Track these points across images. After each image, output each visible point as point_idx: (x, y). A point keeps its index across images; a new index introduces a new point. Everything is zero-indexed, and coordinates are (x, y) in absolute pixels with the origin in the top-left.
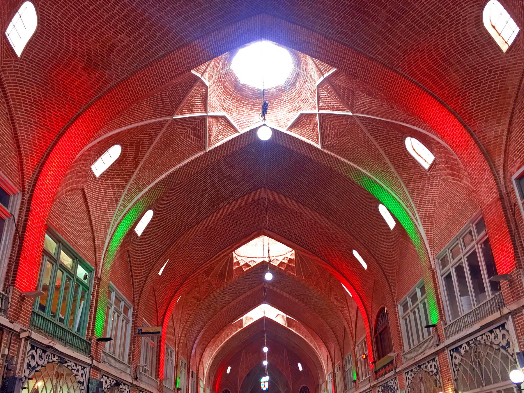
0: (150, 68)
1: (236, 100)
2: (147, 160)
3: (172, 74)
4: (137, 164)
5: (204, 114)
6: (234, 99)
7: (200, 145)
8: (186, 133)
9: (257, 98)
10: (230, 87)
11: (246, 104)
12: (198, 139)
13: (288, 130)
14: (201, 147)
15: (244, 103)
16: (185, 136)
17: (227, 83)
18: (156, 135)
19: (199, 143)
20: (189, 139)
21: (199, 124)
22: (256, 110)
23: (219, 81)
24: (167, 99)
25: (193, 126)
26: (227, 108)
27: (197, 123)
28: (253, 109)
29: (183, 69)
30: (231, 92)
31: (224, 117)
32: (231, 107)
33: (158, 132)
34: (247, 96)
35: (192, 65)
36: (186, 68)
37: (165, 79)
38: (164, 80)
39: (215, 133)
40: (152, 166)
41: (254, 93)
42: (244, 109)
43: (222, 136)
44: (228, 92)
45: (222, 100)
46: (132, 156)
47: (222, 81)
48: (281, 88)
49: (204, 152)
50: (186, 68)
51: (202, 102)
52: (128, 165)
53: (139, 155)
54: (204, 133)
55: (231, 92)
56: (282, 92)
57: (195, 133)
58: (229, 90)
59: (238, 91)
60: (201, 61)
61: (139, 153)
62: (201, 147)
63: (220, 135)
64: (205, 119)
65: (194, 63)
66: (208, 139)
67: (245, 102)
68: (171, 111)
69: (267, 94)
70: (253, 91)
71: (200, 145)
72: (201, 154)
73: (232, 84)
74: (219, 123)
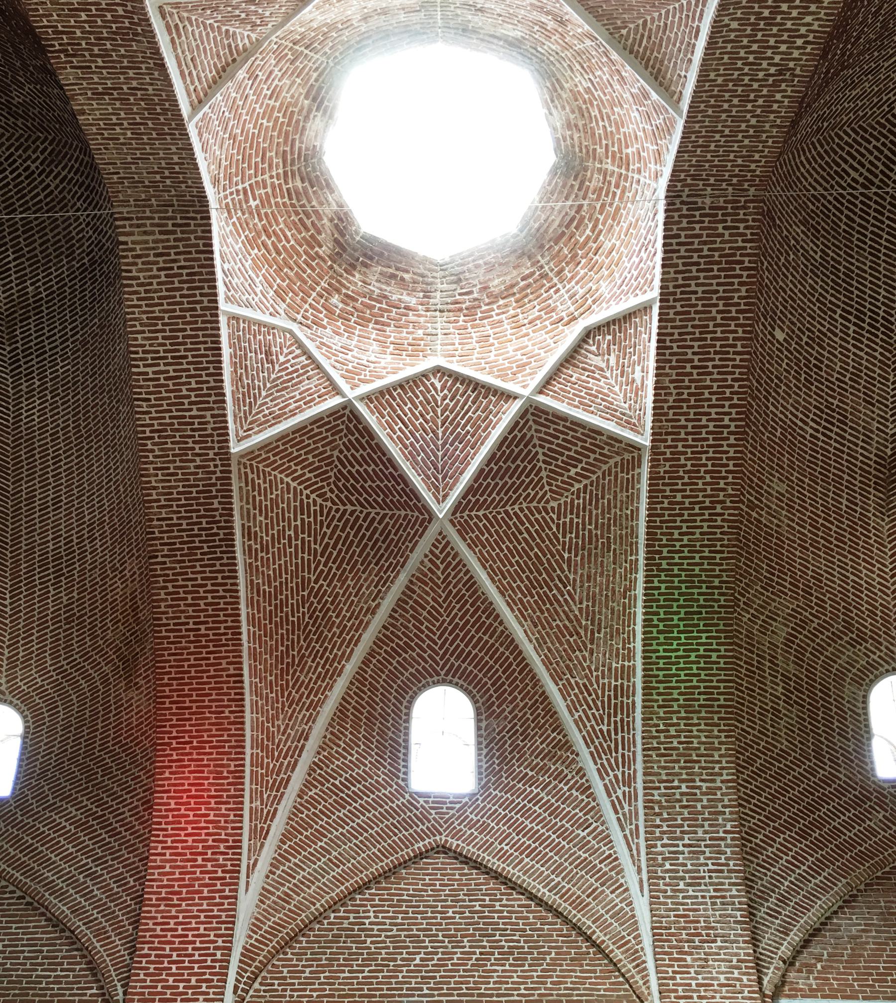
0: (160, 559)
1: (567, 264)
2: (540, 644)
3: (216, 506)
4: (527, 674)
5: (515, 407)
6: (562, 270)
7: (618, 459)
8: (549, 484)
9: (582, 183)
10: (515, 273)
11: (593, 231)
12: (592, 456)
13: (675, 103)
14: (627, 456)
15: (588, 238)
16: (557, 493)
17: (496, 282)
18: (471, 583)
19: (610, 457)
20: (577, 486)
21: (546, 433)
22: (621, 198)
23: (471, 311)
24: (368, 514)
25: (544, 454)
26: (572, 309)
27: (540, 439)
28: (618, 209)
29: (215, 473)
30: (533, 273)
31: (588, 335)
32: (581, 292)
33: (465, 574)
34: (568, 218)
35: (216, 445)
36: (218, 462)
37: (218, 528)
38: (221, 532)
39: (617, 389)
40: (578, 634)
41: (561, 192)
42: (608, 245)
43: (638, 369)
44: (528, 286)
45: (539, 318)
46: (497, 670)
47: (475, 300)
48: (545, 90)
49: (646, 458)
50: (218, 462)
51: (474, 403)
52: (515, 698)
53: (507, 653)
54: (584, 427)
55: (533, 273)
56: (562, 88)
57: (568, 457)
58: (523, 280)
59: (542, 247)
60: (213, 416)
61: (501, 650)
62: (627, 456)
63: (633, 373)
64: (536, 408)
65: (211, 435)
66: (610, 426)
67: (588, 232)
68: (416, 514)
69: (573, 146)
70: (552, 193)
71: (618, 459)
72: (645, 470)
73: (506, 264)
74: (597, 361)
